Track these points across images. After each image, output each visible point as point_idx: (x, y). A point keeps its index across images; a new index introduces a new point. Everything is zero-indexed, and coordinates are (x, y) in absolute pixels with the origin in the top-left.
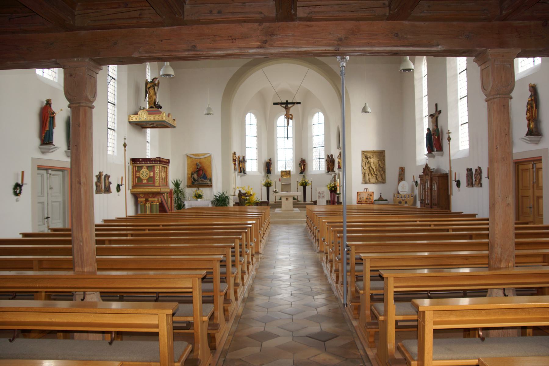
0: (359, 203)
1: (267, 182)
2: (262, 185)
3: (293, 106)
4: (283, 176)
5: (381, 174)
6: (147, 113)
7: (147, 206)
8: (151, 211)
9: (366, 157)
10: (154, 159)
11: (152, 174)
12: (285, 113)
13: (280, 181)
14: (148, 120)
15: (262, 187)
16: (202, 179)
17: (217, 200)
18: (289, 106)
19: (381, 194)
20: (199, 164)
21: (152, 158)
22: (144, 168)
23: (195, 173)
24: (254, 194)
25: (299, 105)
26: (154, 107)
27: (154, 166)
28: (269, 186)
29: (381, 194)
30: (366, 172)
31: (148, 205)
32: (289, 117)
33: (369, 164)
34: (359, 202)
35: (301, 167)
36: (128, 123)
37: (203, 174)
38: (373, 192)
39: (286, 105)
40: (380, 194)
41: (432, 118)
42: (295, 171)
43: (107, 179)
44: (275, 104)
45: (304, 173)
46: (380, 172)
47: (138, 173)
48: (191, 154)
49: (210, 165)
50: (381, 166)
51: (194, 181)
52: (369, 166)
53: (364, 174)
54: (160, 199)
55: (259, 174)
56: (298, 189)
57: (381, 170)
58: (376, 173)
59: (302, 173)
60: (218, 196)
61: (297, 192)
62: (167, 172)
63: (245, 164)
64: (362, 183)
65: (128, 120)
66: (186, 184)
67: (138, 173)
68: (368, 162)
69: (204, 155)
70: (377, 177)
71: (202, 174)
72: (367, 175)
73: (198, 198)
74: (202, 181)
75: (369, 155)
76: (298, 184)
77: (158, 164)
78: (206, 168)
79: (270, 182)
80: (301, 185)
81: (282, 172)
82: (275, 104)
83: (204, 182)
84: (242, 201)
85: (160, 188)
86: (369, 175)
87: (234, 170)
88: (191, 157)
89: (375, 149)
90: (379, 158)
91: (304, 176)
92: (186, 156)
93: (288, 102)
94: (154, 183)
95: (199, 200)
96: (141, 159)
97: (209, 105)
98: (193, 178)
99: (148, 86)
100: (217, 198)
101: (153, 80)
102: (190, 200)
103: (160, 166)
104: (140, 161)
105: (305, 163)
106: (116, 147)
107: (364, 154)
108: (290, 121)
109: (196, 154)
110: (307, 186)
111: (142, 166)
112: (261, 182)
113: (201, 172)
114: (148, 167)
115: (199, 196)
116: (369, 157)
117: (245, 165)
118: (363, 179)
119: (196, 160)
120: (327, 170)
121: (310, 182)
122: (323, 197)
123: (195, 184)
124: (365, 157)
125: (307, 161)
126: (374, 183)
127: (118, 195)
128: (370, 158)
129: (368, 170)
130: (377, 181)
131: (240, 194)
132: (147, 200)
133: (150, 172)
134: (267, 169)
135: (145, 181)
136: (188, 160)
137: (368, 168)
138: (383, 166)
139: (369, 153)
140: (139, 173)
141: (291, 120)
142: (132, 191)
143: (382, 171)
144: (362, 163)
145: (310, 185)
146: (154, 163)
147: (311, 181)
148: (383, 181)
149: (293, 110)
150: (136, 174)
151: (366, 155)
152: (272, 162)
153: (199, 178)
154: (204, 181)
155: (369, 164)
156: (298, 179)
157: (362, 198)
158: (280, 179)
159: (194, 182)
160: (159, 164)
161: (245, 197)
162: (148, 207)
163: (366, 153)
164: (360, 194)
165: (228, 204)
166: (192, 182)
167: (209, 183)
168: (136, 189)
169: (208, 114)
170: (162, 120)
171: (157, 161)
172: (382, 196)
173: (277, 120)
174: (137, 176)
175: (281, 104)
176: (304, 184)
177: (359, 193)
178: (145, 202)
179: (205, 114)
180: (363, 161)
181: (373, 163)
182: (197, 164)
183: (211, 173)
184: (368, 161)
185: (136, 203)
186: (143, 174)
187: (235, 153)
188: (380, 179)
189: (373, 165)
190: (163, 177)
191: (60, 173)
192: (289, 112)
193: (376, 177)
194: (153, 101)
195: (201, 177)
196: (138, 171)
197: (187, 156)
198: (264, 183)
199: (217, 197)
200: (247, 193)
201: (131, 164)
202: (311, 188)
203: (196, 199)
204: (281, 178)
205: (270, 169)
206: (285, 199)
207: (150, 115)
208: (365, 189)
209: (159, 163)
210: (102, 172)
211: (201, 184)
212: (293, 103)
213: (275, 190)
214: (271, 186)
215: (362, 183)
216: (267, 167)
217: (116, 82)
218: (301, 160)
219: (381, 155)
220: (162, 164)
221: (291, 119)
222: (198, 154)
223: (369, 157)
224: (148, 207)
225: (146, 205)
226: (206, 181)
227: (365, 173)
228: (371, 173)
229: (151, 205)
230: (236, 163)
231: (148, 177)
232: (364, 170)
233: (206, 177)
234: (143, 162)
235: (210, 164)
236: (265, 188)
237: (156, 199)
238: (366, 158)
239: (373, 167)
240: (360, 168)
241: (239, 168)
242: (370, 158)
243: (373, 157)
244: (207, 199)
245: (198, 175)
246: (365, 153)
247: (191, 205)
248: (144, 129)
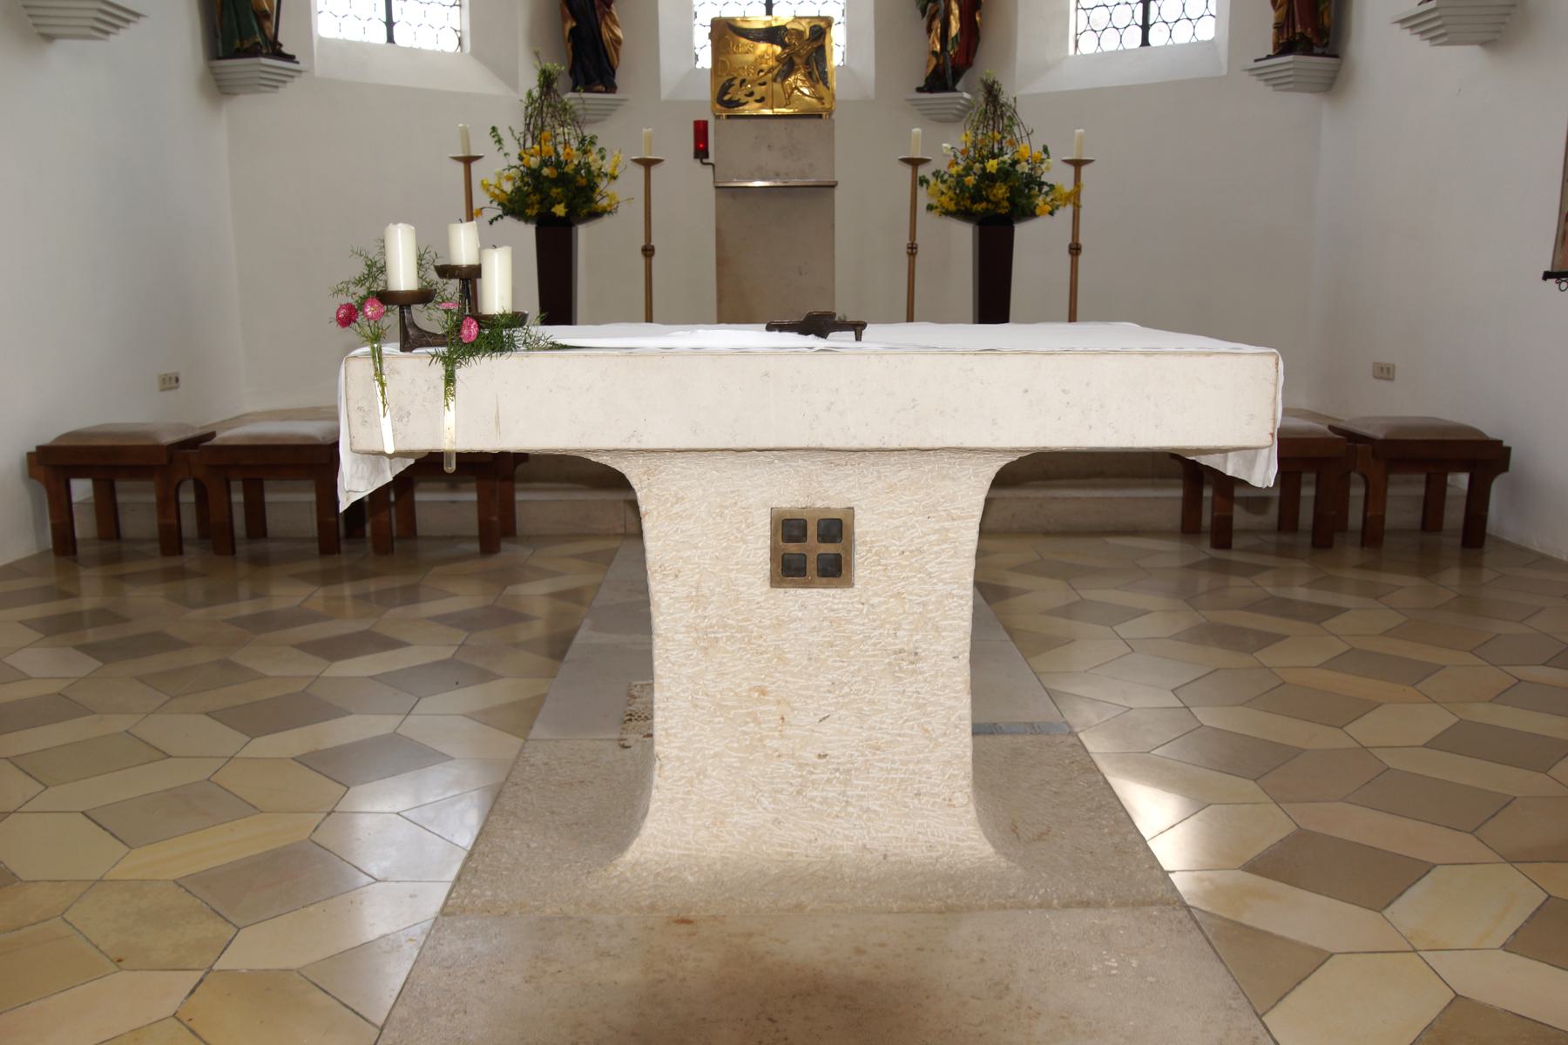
1: (534, 162)
4: (736, 93)
13: (701, 152)
28: (560, 210)
42: (867, 66)
45: (959, 86)
55: (478, 81)
56: (912, 250)
59: (940, 80)
76: (922, 192)
80: (963, 214)
81: (725, 32)
91: (992, 92)
110: (1029, 213)
112: (468, 161)
120: (1279, 27)
121: (1057, 174)
134: (572, 31)
145: (1065, 213)
147: (1078, 164)
156: (917, 139)
158: (701, 130)
176: (1001, 191)
202: (1075, 250)
205: (606, 35)
213: (403, 278)
214: (596, 215)
216: (574, 16)
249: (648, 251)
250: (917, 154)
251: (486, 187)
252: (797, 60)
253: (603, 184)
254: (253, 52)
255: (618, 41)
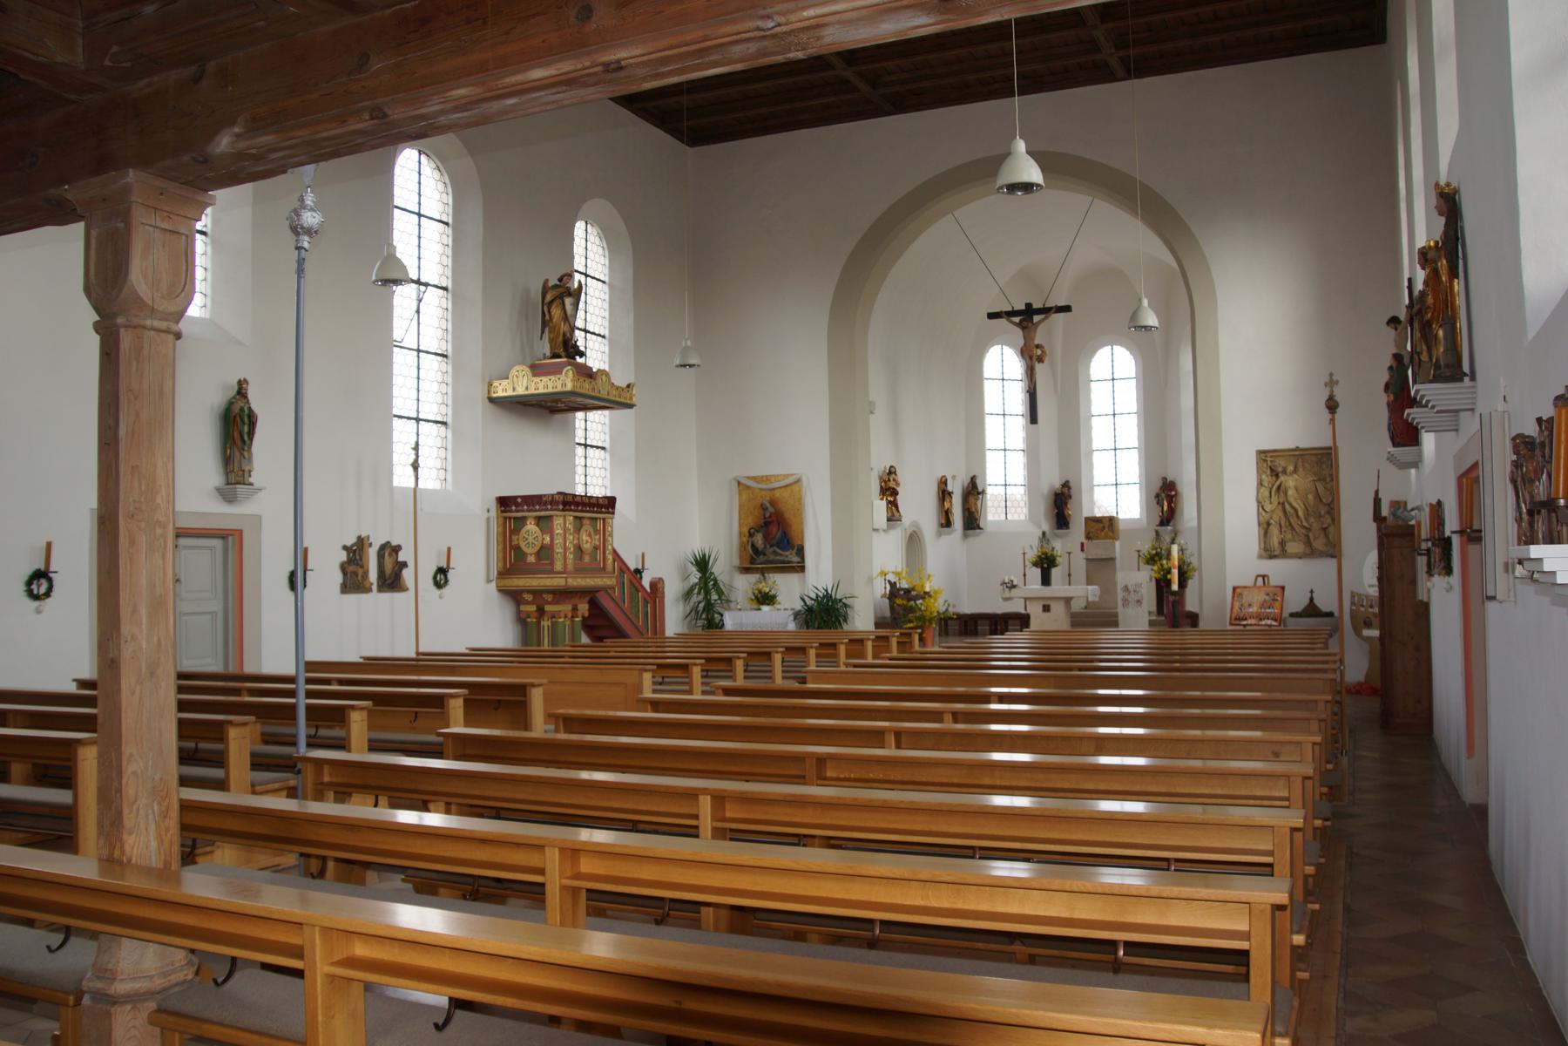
0: (1237, 622)
2: (1027, 563)
3: (1046, 318)
4: (1091, 535)
5: (1325, 526)
6: (530, 374)
7: (544, 627)
8: (553, 642)
9: (1272, 470)
10: (550, 498)
11: (548, 539)
12: (1021, 342)
13: (1082, 550)
14: (532, 391)
15: (1027, 569)
16: (775, 548)
17: (810, 610)
18: (1036, 318)
19: (1314, 595)
20: (768, 505)
21: (545, 495)
22: (528, 523)
23: (758, 532)
24: (936, 592)
25: (1061, 315)
26: (563, 354)
27: (550, 518)
28: (1045, 566)
29: (1312, 592)
30: (1272, 521)
31: (546, 623)
32: (1032, 356)
33: (1282, 494)
34: (1236, 619)
35: (1160, 503)
36: (487, 401)
37: (779, 534)
38: (1283, 588)
39: (1027, 316)
40: (1309, 595)
41: (1396, 329)
43: (387, 554)
44: (992, 316)
45: (1171, 524)
46: (1322, 519)
47: (515, 538)
48: (748, 478)
49: (799, 511)
50: (1324, 500)
51: (755, 554)
52: (1281, 500)
53: (1265, 526)
54: (584, 608)
57: (1323, 512)
58: (1306, 524)
60: (814, 596)
61: (1067, 587)
62: (605, 535)
63: (977, 500)
64: (1260, 557)
65: (486, 395)
66: (736, 562)
67: (515, 538)
68: (1279, 487)
69: (784, 480)
70: (1311, 535)
71: (776, 533)
72: (1274, 531)
73: (763, 604)
74: (775, 552)
75: (1281, 463)
77: (559, 510)
78: (787, 516)
79: (1050, 553)
82: (992, 316)
83: (781, 558)
84: (898, 614)
85: (566, 578)
86: (1281, 531)
87: (889, 520)
88: (748, 487)
89: (1304, 443)
90: (1315, 474)
92: (736, 484)
93: (1035, 307)
94: (552, 563)
95: (765, 608)
96: (523, 497)
97: (686, 340)
98: (753, 546)
99: (549, 298)
100: (809, 602)
101: (560, 280)
102: (740, 610)
103: (565, 516)
104: (517, 505)
105: (1173, 493)
106: (449, 468)
107: (1265, 461)
108: (1038, 366)
109: (762, 477)
111: (524, 519)
112: (1024, 554)
113: (774, 529)
114: (539, 520)
115: (765, 599)
116: (1280, 469)
117: (979, 502)
118: (1262, 547)
119: (763, 493)
122: (1139, 602)
123: (758, 561)
124: (1269, 472)
125: (1179, 487)
126: (1300, 558)
127: (441, 597)
128: (1284, 472)
129: (1279, 513)
130: (1308, 551)
131: (894, 592)
132: (541, 612)
133: (543, 532)
135: (531, 559)
136: (740, 494)
137: (1280, 507)
138: (1330, 499)
139: (1283, 456)
140: (517, 537)
141: (1039, 362)
142: (502, 584)
143: (1327, 516)
144: (1258, 492)
146: (551, 510)
148: (1333, 550)
149: (1051, 331)
150: (511, 541)
151: (1271, 464)
152: (1073, 492)
153: (768, 547)
154: (781, 555)
155: (1282, 494)
157: (1246, 605)
158: (1082, 545)
159: (754, 556)
160: (563, 510)
161: (909, 600)
162: (546, 627)
163: (1271, 457)
164: (1241, 594)
165: (845, 621)
166: (751, 556)
167: (796, 559)
168: (509, 580)
169: (684, 366)
170: (565, 389)
171: (557, 503)
172: (1316, 601)
173: (1090, 361)
174: (513, 543)
175: (1010, 314)
177: (1238, 591)
178: (536, 614)
179: (677, 366)
180: (1260, 484)
181: (1296, 489)
182: (762, 505)
183: (802, 532)
184: (1278, 483)
185: (521, 620)
186: (527, 539)
187: (893, 470)
188: (1319, 544)
189: (1296, 495)
190: (587, 547)
191: (217, 543)
192: (1033, 340)
193: (1307, 536)
194: (561, 338)
195: (774, 542)
196: (516, 531)
197: (739, 483)
198: (1032, 554)
199: (812, 599)
200: (913, 589)
201: (499, 512)
203: (756, 607)
204: (1085, 541)
205: (1066, 513)
206: (1041, 609)
207: (537, 379)
208: (1258, 576)
209: (561, 507)
210: (368, 537)
211: (772, 562)
212: (1046, 311)
213: (1007, 581)
215: (1260, 557)
217: (450, 296)
218: (1160, 484)
219: (1322, 462)
220: (571, 510)
221: (1040, 360)
222: (767, 476)
223: (1280, 469)
224: (546, 627)
225: (542, 623)
226: (787, 553)
227: (1269, 524)
228: (1290, 524)
229: (552, 623)
230: (895, 499)
231: (540, 545)
232: (1264, 513)
233: (788, 541)
234: (523, 506)
235: (800, 504)
236: (1038, 572)
237: (566, 608)
238: (1272, 476)
239: (1295, 504)
240: (1255, 505)
241: (944, 513)
242: (1284, 472)
243: (1295, 471)
244: (786, 607)
245: (766, 538)
246: (1269, 459)
247: (741, 624)
248: (558, 417)
249: (1069, 575)
250: (1138, 549)
251: (1028, 560)
252: (1107, 526)
253: (1058, 558)
254: (974, 529)
255: (1069, 515)
